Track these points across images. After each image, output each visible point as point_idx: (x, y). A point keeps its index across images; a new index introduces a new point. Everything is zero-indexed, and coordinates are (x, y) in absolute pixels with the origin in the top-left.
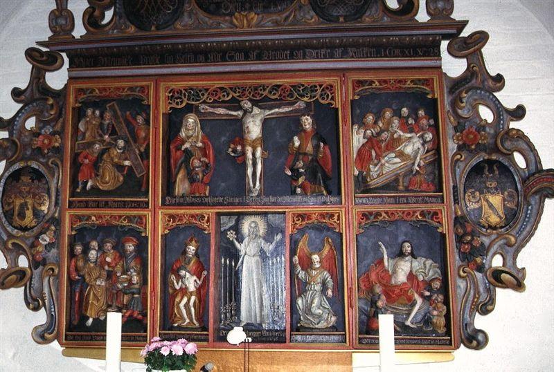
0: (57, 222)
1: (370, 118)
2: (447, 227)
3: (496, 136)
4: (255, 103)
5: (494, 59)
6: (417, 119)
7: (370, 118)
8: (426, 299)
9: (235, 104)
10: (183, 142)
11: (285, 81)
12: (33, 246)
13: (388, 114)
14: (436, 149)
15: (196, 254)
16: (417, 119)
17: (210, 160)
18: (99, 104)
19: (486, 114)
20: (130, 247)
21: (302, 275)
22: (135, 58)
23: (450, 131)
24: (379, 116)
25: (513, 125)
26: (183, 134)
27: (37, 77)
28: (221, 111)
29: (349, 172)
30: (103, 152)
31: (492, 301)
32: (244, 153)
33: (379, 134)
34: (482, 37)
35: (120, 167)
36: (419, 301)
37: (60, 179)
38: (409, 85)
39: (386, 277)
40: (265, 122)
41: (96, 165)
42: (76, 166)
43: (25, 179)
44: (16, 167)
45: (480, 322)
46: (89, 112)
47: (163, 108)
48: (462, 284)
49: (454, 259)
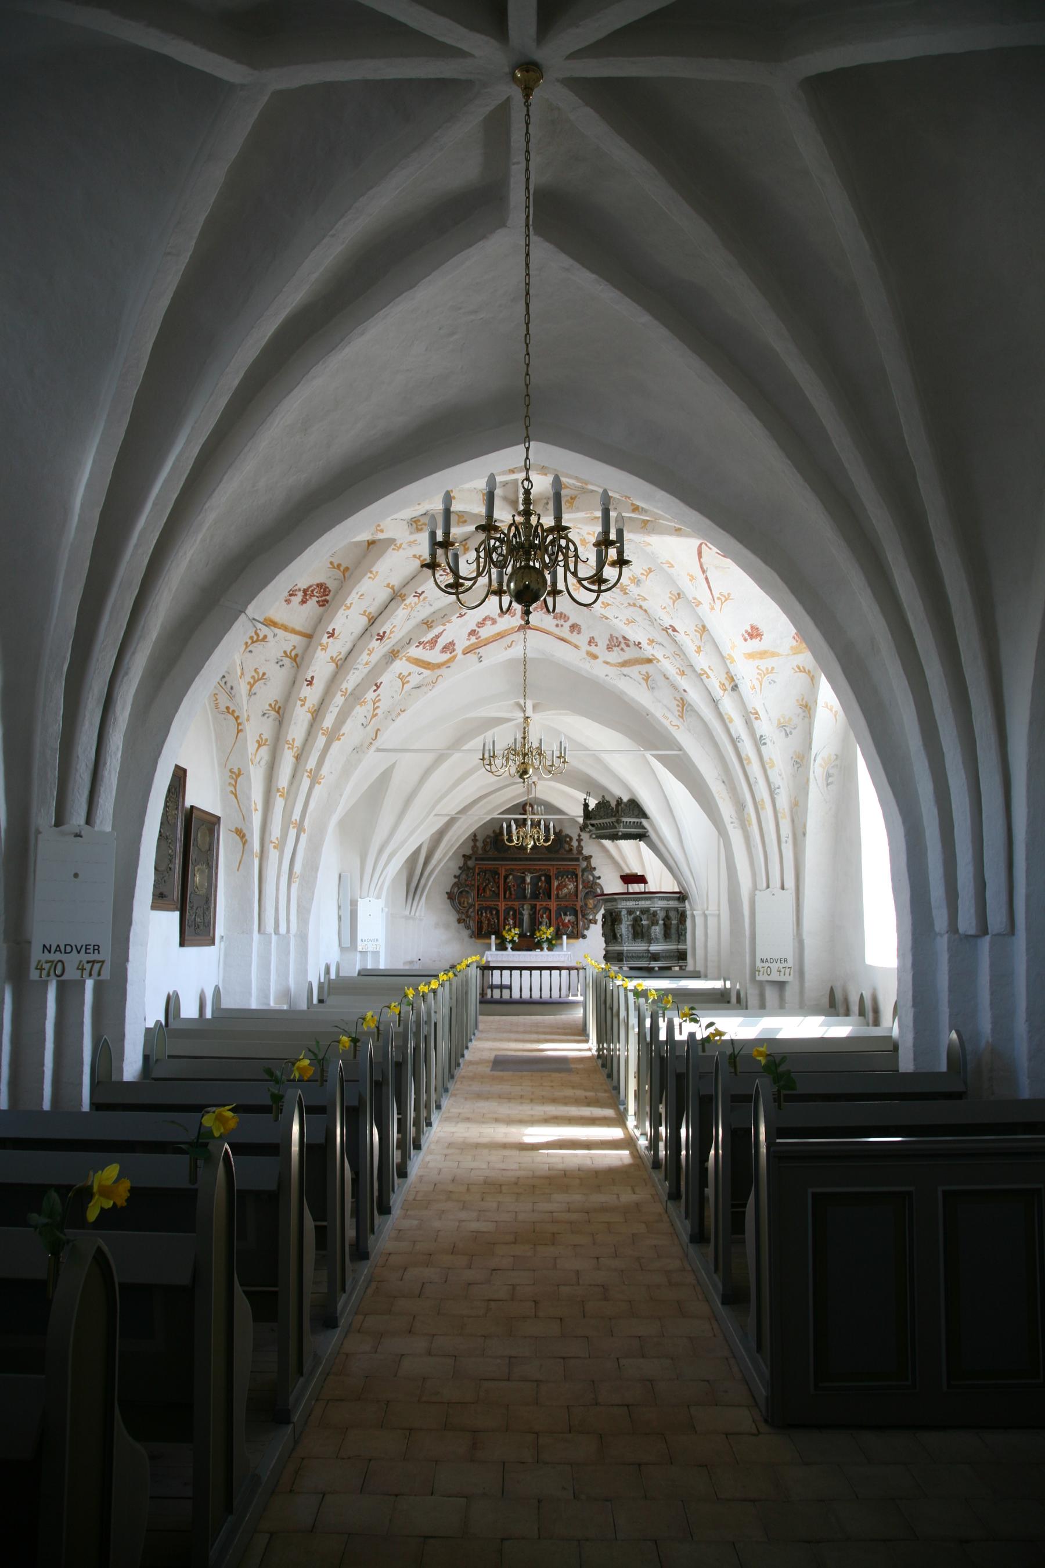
0: (474, 905)
1: (560, 878)
2: (578, 908)
3: (592, 884)
4: (529, 873)
5: (594, 863)
6: (572, 878)
7: (560, 878)
8: (573, 927)
9: (523, 873)
10: (508, 883)
11: (537, 868)
12: (467, 912)
13: (565, 877)
14: (577, 887)
15: (513, 915)
16: (572, 878)
17: (515, 888)
18: (485, 872)
19: (591, 878)
20: (494, 912)
21: (540, 920)
22: (495, 859)
23: (581, 883)
24: (562, 877)
25: (598, 881)
26: (508, 880)
27: (465, 863)
28: (519, 874)
29: (554, 892)
30: (486, 885)
31: (589, 927)
32: (525, 886)
33: (562, 883)
34: (591, 857)
35: (491, 890)
36: (571, 927)
37: (473, 894)
38: (571, 870)
39: (563, 921)
40: (531, 878)
41: (484, 890)
42: (478, 891)
43: (464, 893)
44: (461, 890)
45: (586, 932)
46: (481, 873)
47: (503, 874)
48: (581, 923)
49: (580, 916)
